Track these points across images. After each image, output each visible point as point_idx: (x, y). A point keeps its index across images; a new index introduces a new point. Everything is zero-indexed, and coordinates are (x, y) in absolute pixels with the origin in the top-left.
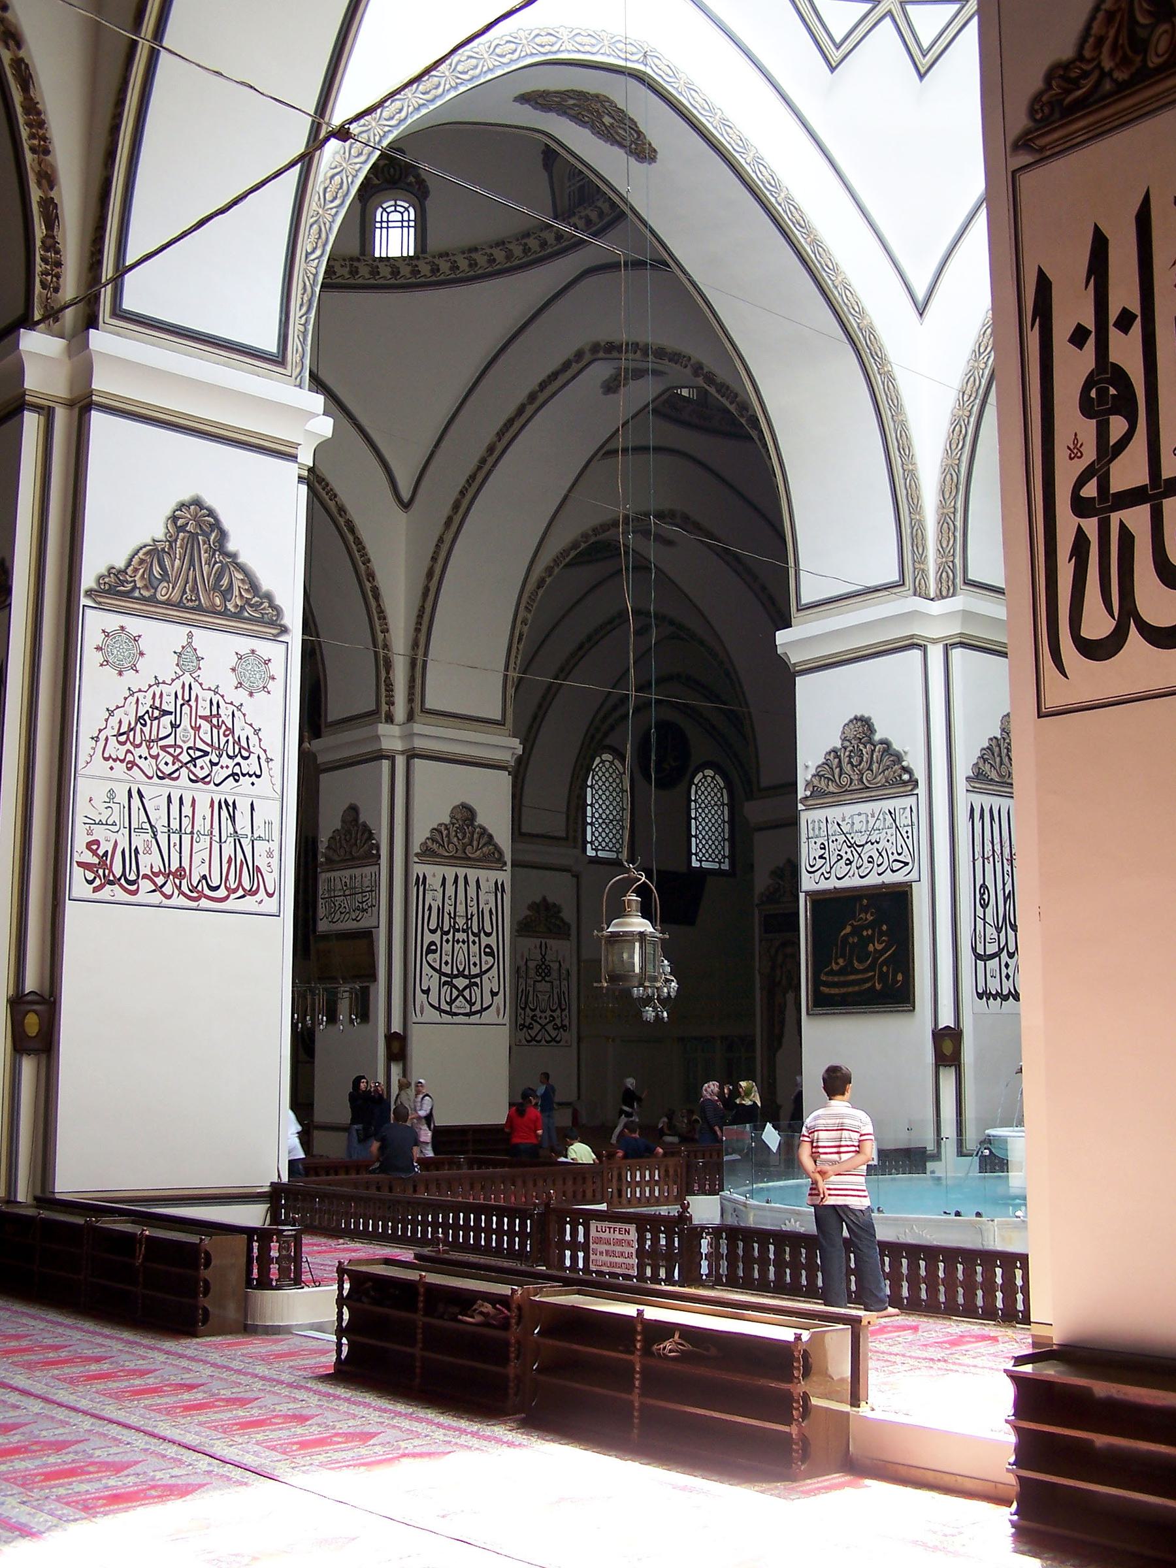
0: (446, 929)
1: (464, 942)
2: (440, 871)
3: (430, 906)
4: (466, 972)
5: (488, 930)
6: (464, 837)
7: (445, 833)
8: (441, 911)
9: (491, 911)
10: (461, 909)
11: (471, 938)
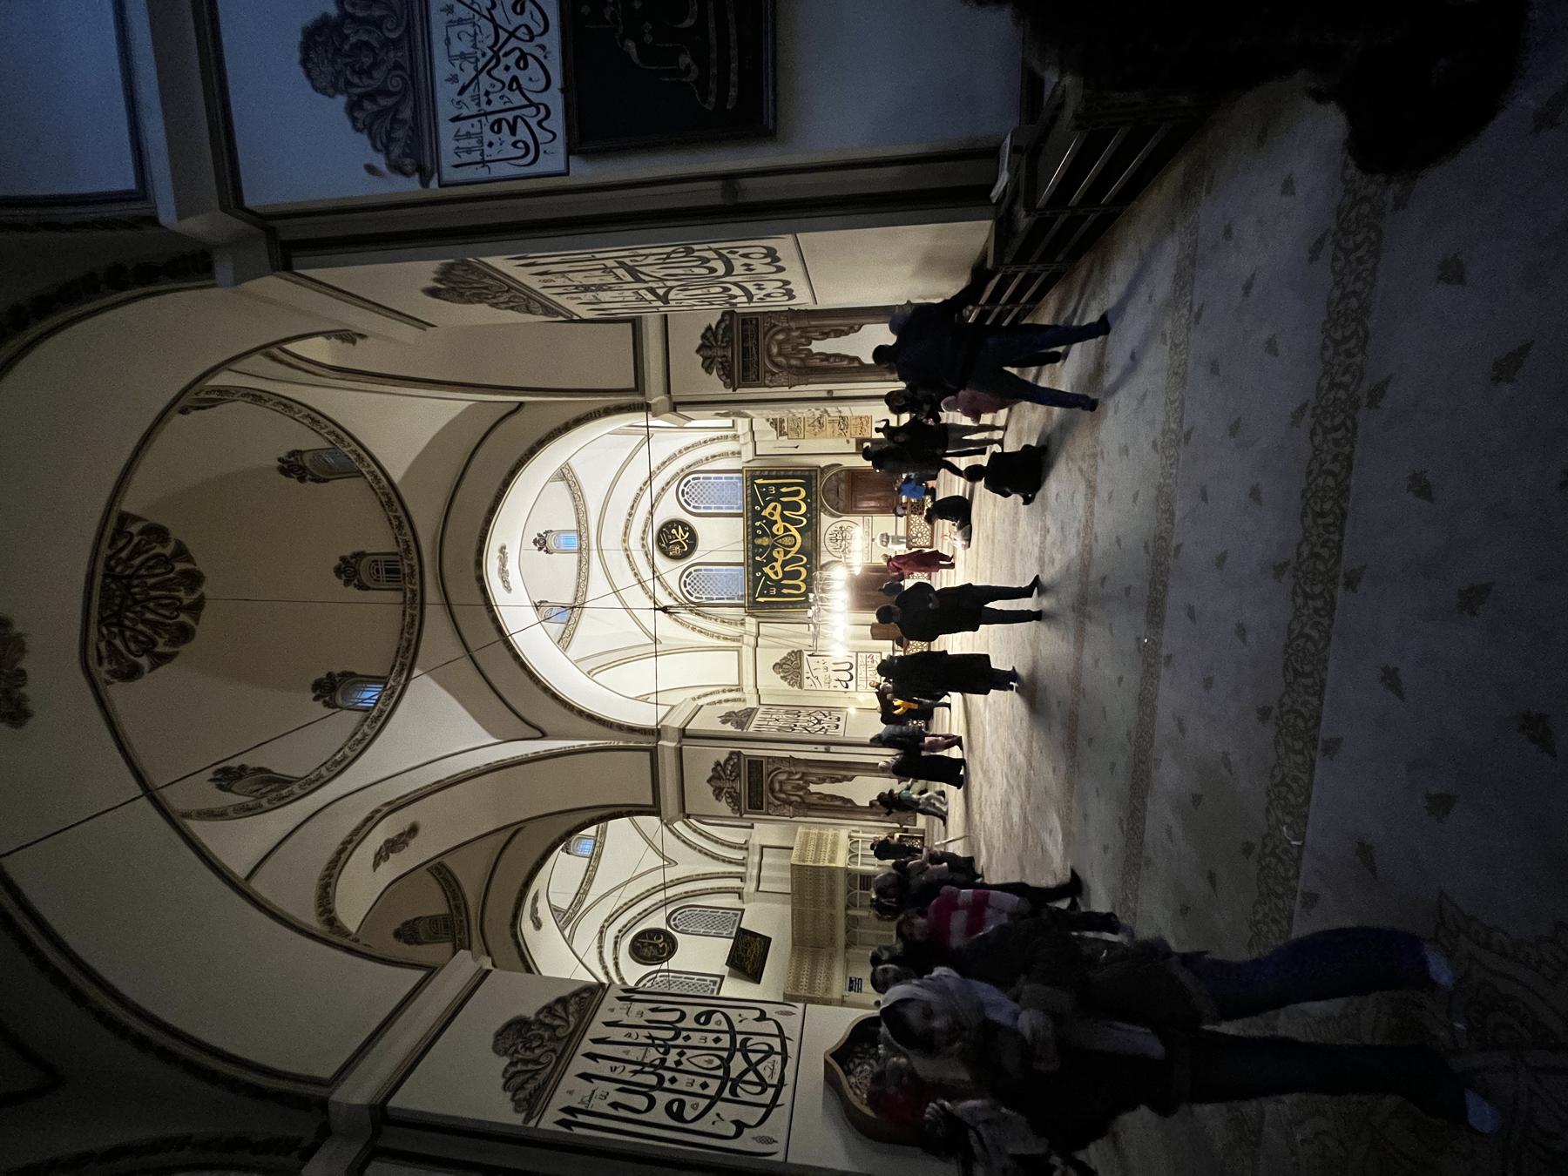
0: (653, 1080)
1: (681, 1054)
2: (569, 1080)
3: (615, 1105)
4: (725, 1054)
5: (677, 1015)
6: (542, 1038)
7: (520, 1067)
8: (627, 1087)
9: (653, 1010)
10: (635, 1053)
11: (680, 1042)
